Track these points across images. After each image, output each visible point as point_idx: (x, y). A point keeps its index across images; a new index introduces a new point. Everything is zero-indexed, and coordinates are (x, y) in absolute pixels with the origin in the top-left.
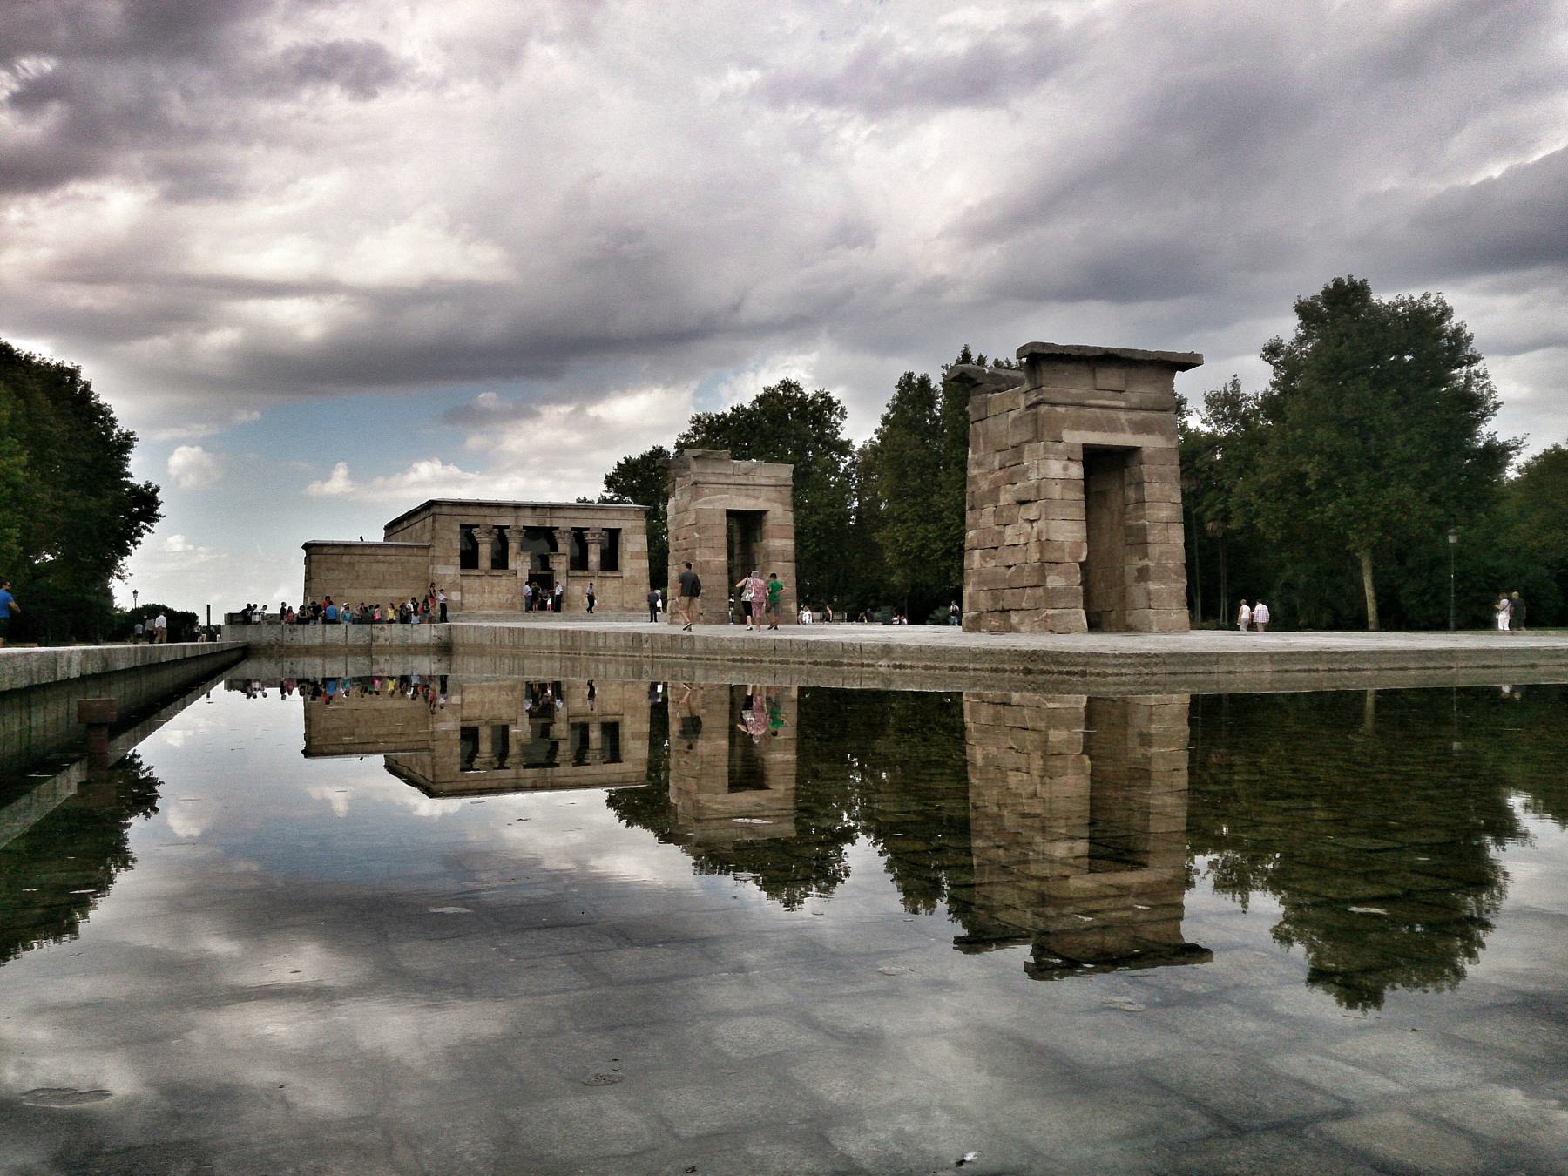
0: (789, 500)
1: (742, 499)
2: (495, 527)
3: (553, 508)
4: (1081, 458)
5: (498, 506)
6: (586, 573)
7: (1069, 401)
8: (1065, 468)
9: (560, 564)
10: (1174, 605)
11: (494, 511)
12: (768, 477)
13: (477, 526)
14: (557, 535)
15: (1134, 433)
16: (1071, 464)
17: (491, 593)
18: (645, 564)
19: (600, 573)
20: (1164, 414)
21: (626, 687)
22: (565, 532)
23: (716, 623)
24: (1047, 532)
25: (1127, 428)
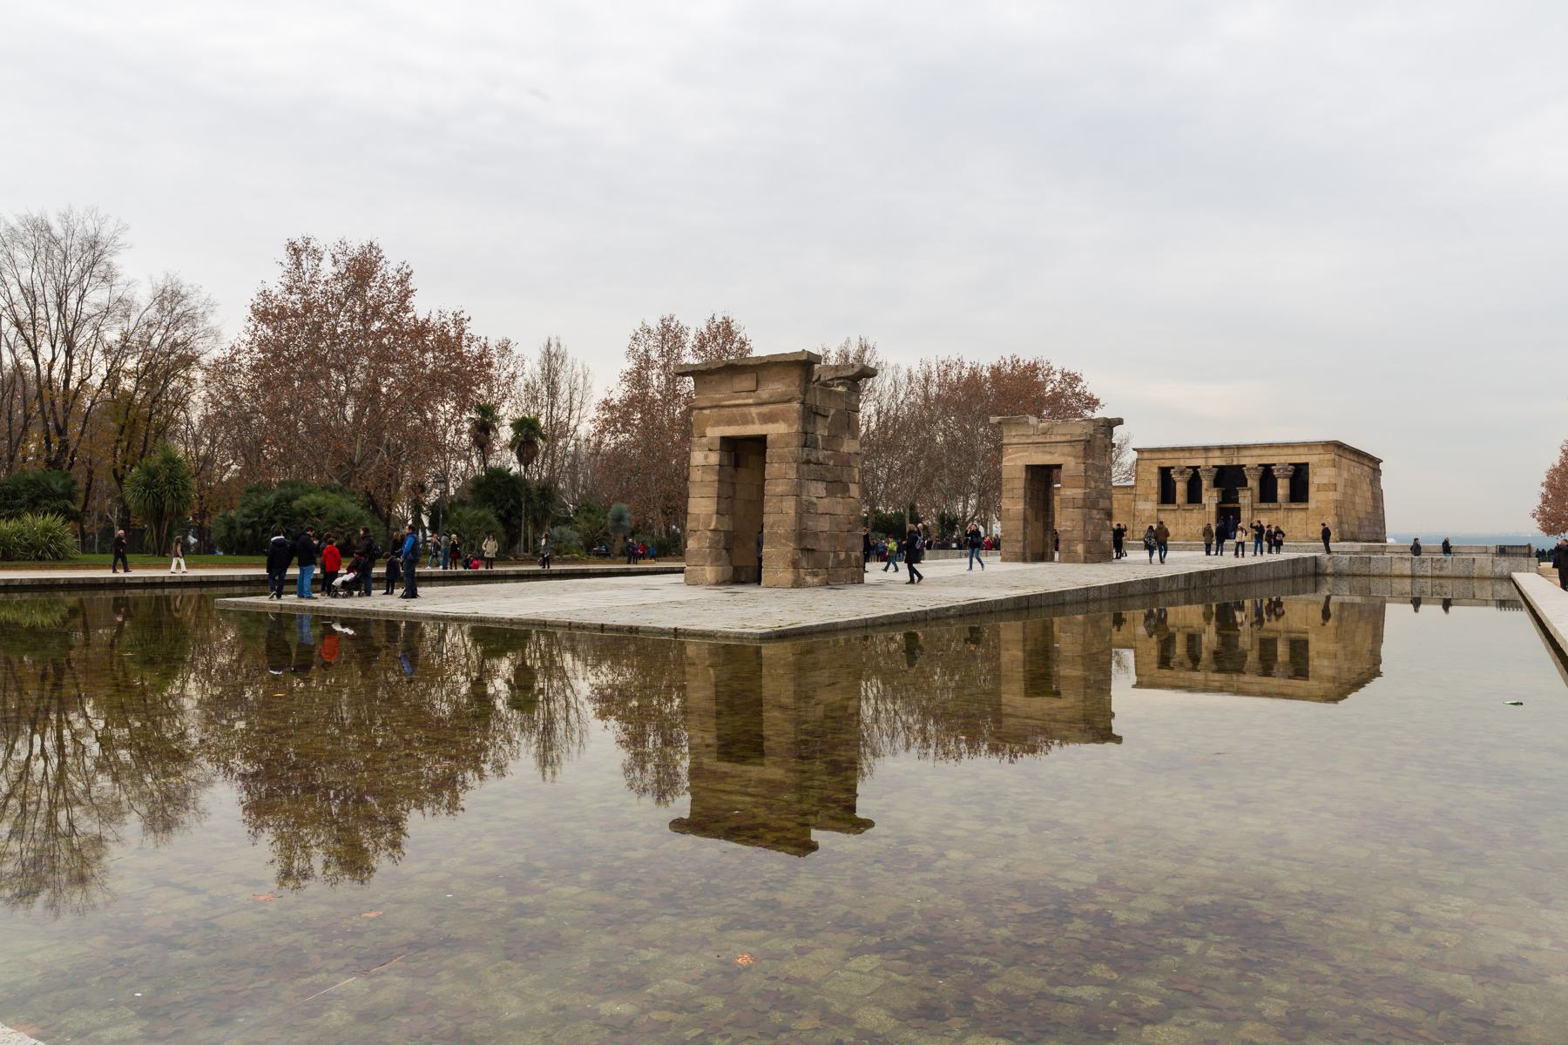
1: (1040, 455)
3: (1239, 448)
5: (1190, 449)
7: (709, 404)
8: (706, 457)
9: (1246, 498)
10: (781, 565)
11: (1188, 455)
12: (1064, 435)
14: (1246, 472)
17: (1184, 524)
19: (1284, 505)
20: (788, 405)
21: (1310, 607)
22: (1249, 469)
25: (756, 421)
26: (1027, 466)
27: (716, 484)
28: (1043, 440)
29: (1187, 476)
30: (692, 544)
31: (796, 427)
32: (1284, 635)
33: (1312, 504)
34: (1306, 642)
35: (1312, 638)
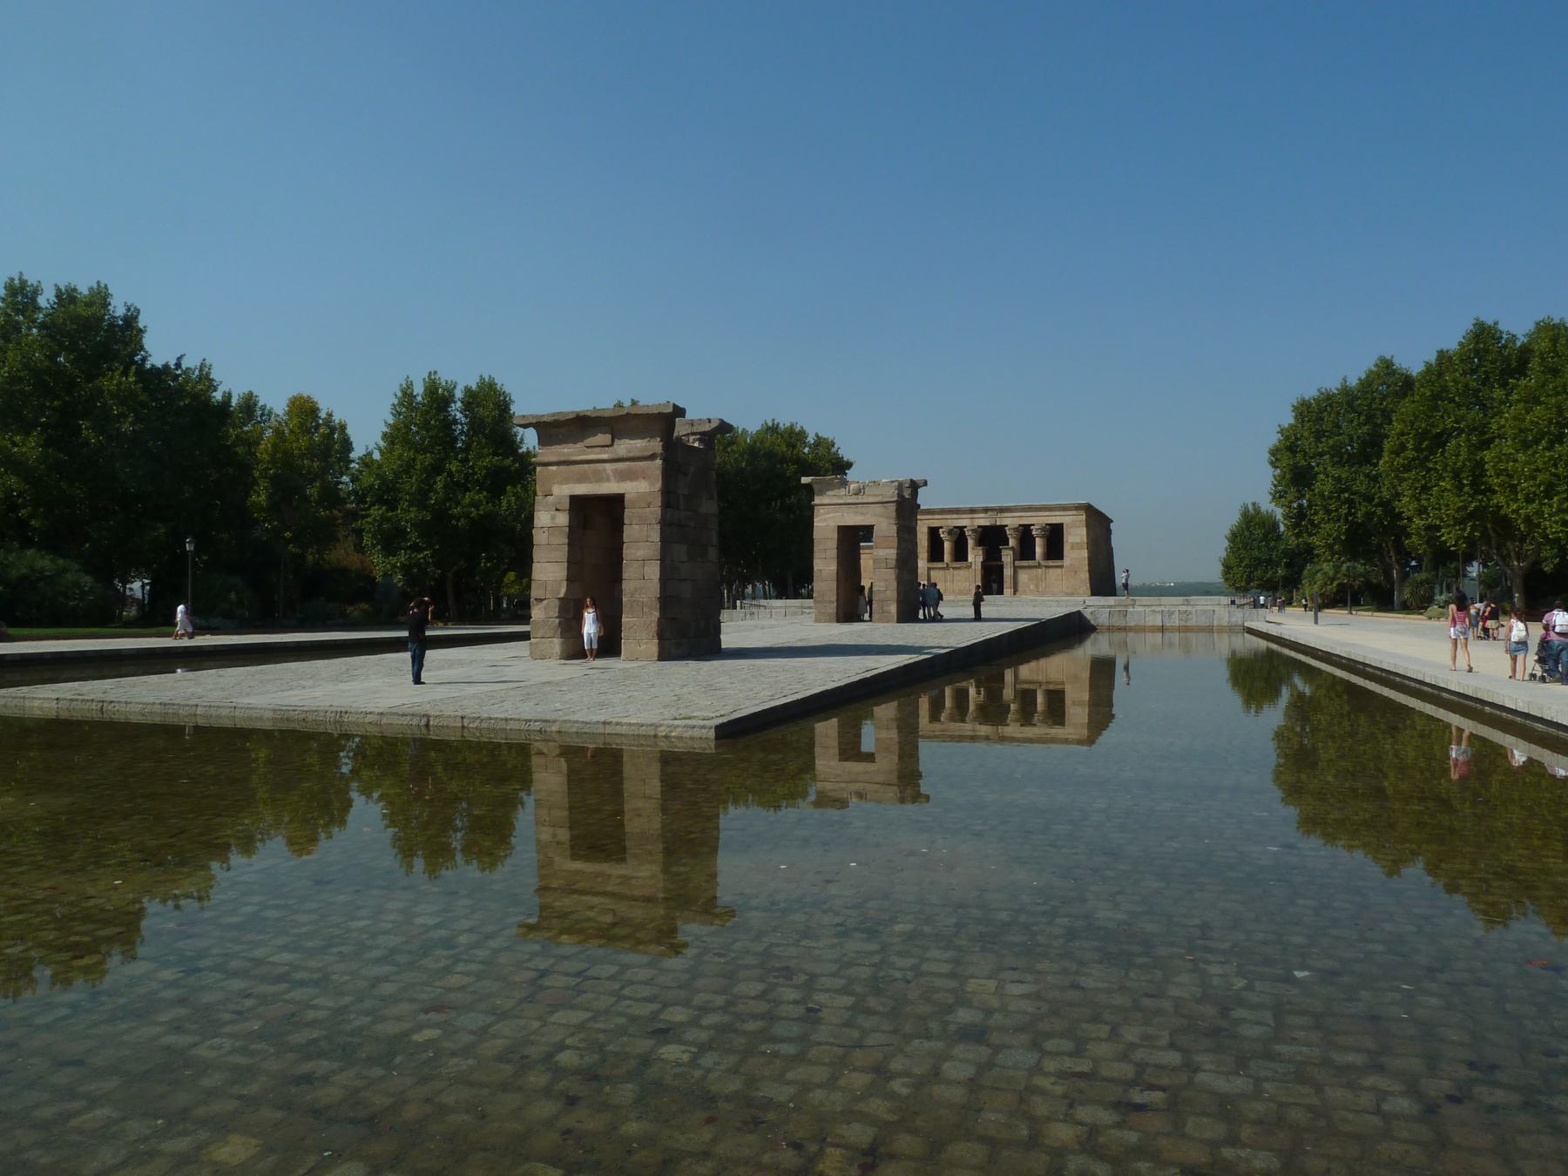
0: (894, 514)
2: (955, 527)
3: (1002, 510)
4: (568, 508)
5: (957, 511)
6: (1031, 563)
8: (553, 518)
9: (1007, 557)
12: (874, 495)
13: (942, 528)
14: (1008, 532)
15: (618, 482)
16: (558, 513)
18: (1085, 553)
19: (1043, 563)
23: (825, 622)
24: (868, 548)
25: (612, 478)
26: (839, 526)
27: (566, 548)
28: (857, 501)
29: (955, 537)
30: (537, 613)
31: (659, 485)
32: (1044, 687)
33: (1067, 561)
34: (1062, 692)
35: (1068, 689)
